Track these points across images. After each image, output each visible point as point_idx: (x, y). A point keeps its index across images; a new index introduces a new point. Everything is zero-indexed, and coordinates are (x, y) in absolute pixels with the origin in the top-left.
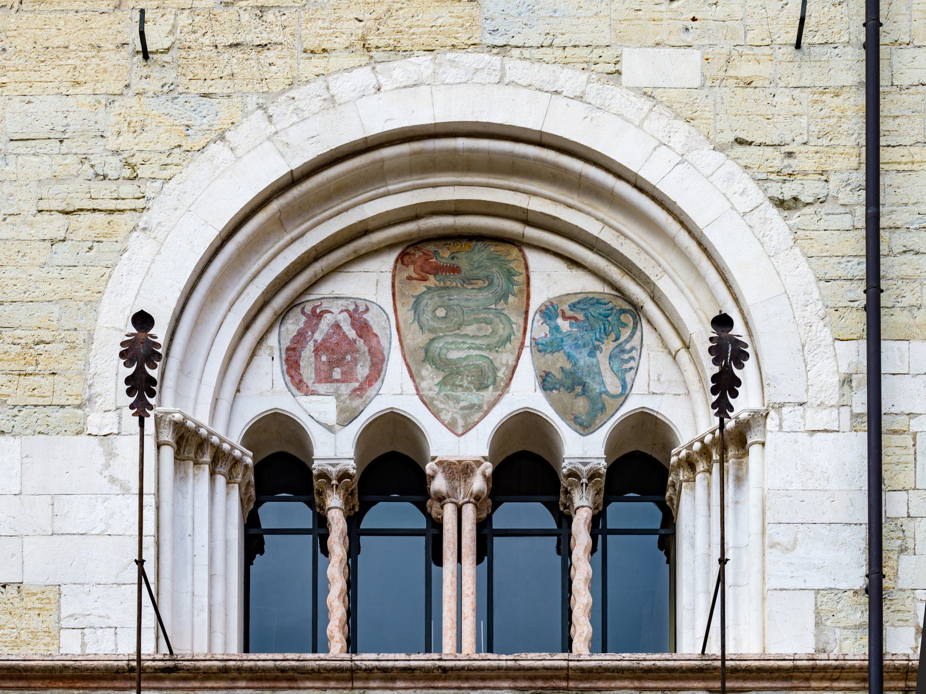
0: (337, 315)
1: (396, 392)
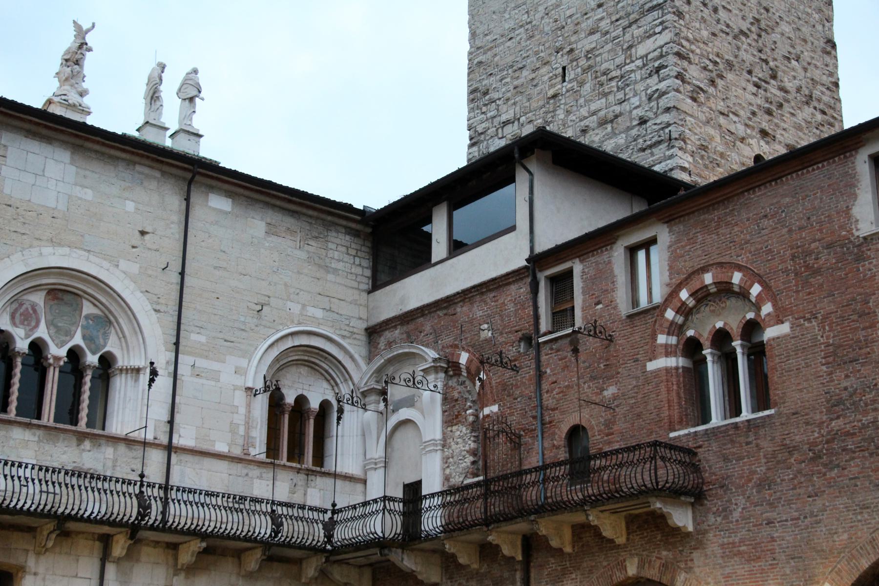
1: (42, 332)
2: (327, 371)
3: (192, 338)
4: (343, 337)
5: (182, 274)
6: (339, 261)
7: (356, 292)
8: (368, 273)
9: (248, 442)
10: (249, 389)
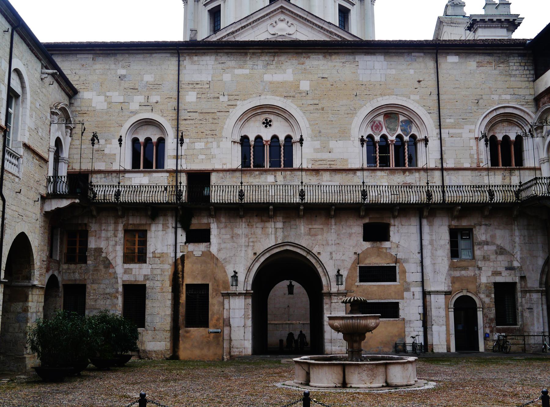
0: (377, 122)
1: (384, 131)
2: (517, 122)
3: (447, 121)
4: (522, 105)
5: (438, 94)
6: (516, 70)
7: (527, 83)
8: (532, 72)
9: (479, 161)
10: (476, 138)
